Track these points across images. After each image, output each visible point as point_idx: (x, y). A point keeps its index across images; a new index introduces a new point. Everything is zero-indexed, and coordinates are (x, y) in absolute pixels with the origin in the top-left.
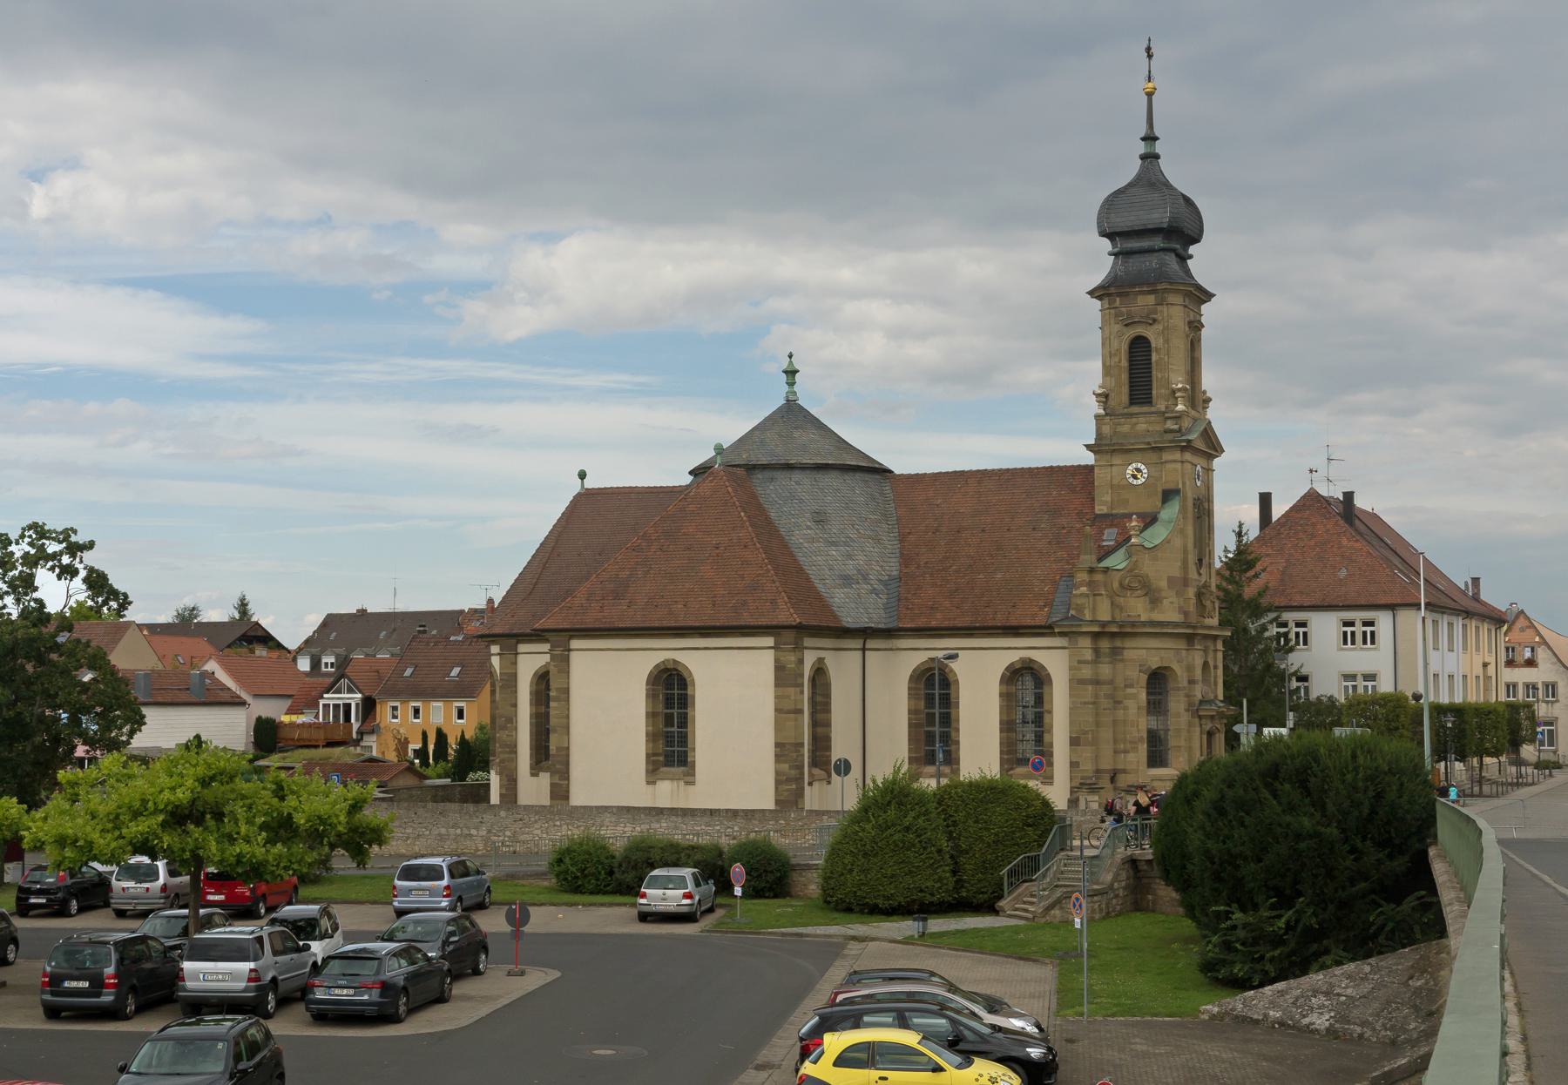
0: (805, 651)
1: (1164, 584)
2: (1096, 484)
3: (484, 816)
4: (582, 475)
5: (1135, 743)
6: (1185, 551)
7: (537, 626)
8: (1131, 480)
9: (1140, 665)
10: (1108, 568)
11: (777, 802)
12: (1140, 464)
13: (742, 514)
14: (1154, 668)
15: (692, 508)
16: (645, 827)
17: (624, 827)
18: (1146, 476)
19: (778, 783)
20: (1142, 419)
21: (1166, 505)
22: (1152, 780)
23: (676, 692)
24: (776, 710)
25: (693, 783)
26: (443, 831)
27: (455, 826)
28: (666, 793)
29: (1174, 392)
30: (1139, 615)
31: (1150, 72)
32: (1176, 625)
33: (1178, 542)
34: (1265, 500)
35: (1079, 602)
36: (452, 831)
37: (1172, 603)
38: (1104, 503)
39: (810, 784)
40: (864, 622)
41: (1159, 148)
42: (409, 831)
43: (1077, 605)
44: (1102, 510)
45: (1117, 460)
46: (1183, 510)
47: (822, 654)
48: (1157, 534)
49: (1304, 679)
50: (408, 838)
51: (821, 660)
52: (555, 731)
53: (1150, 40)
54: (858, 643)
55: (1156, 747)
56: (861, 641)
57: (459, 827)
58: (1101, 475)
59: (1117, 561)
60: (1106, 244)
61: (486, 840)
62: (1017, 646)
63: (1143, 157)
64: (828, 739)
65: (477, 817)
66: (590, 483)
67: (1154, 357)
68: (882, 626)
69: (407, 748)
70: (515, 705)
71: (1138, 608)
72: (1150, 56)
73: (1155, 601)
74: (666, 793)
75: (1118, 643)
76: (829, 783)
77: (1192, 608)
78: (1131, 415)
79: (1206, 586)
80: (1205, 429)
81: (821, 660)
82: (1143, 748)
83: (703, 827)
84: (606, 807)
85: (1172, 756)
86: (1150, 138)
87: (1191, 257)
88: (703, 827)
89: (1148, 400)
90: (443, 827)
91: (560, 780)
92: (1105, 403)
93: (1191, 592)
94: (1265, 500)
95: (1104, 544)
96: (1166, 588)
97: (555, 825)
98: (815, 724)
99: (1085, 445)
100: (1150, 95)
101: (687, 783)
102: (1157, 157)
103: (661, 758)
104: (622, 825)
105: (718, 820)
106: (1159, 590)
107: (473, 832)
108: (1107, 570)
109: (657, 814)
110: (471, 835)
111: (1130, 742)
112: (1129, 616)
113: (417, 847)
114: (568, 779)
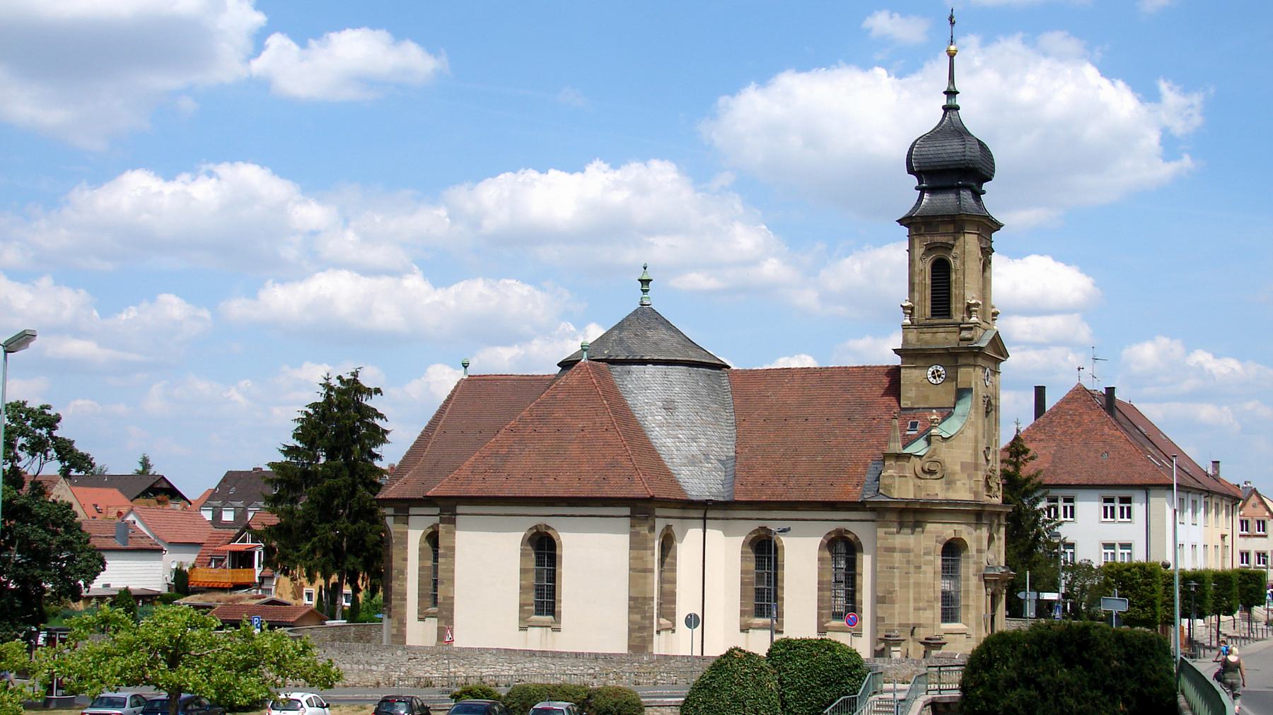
0: (656, 519)
1: (958, 468)
2: (902, 382)
3: (383, 654)
4: (465, 366)
5: (931, 602)
6: (976, 441)
7: (429, 494)
8: (931, 380)
9: (937, 537)
10: (911, 454)
11: (630, 647)
12: (939, 367)
13: (605, 402)
14: (948, 539)
15: (560, 396)
18: (944, 376)
19: (631, 631)
21: (960, 402)
23: (546, 552)
24: (630, 569)
25: (559, 630)
27: (358, 662)
28: (536, 639)
29: (969, 306)
31: (952, 37)
32: (967, 503)
33: (970, 433)
34: (1040, 392)
35: (886, 483)
36: (355, 666)
37: (964, 484)
38: (909, 399)
39: (658, 632)
40: (706, 496)
41: (959, 100)
43: (885, 484)
44: (906, 404)
46: (976, 406)
47: (670, 522)
48: (950, 427)
49: (1072, 546)
51: (668, 527)
52: (443, 583)
53: (952, 10)
54: (699, 513)
55: (948, 605)
56: (703, 512)
57: (361, 663)
58: (906, 375)
59: (919, 447)
60: (914, 180)
63: (947, 109)
64: (673, 594)
65: (377, 655)
67: (953, 276)
68: (721, 499)
69: (302, 591)
70: (405, 559)
71: (936, 490)
72: (952, 23)
73: (950, 483)
74: (536, 639)
75: (919, 518)
76: (674, 631)
77: (981, 488)
78: (932, 326)
79: (993, 471)
80: (994, 338)
81: (668, 527)
82: (938, 606)
84: (488, 649)
85: (962, 612)
86: (951, 93)
87: (984, 193)
89: (948, 314)
90: (348, 663)
92: (911, 315)
93: (981, 476)
94: (1040, 392)
95: (908, 433)
96: (960, 472)
98: (662, 581)
99: (894, 350)
100: (952, 56)
101: (554, 630)
102: (957, 108)
103: (533, 608)
106: (954, 474)
107: (374, 668)
108: (909, 456)
109: (531, 656)
111: (928, 601)
112: (928, 495)
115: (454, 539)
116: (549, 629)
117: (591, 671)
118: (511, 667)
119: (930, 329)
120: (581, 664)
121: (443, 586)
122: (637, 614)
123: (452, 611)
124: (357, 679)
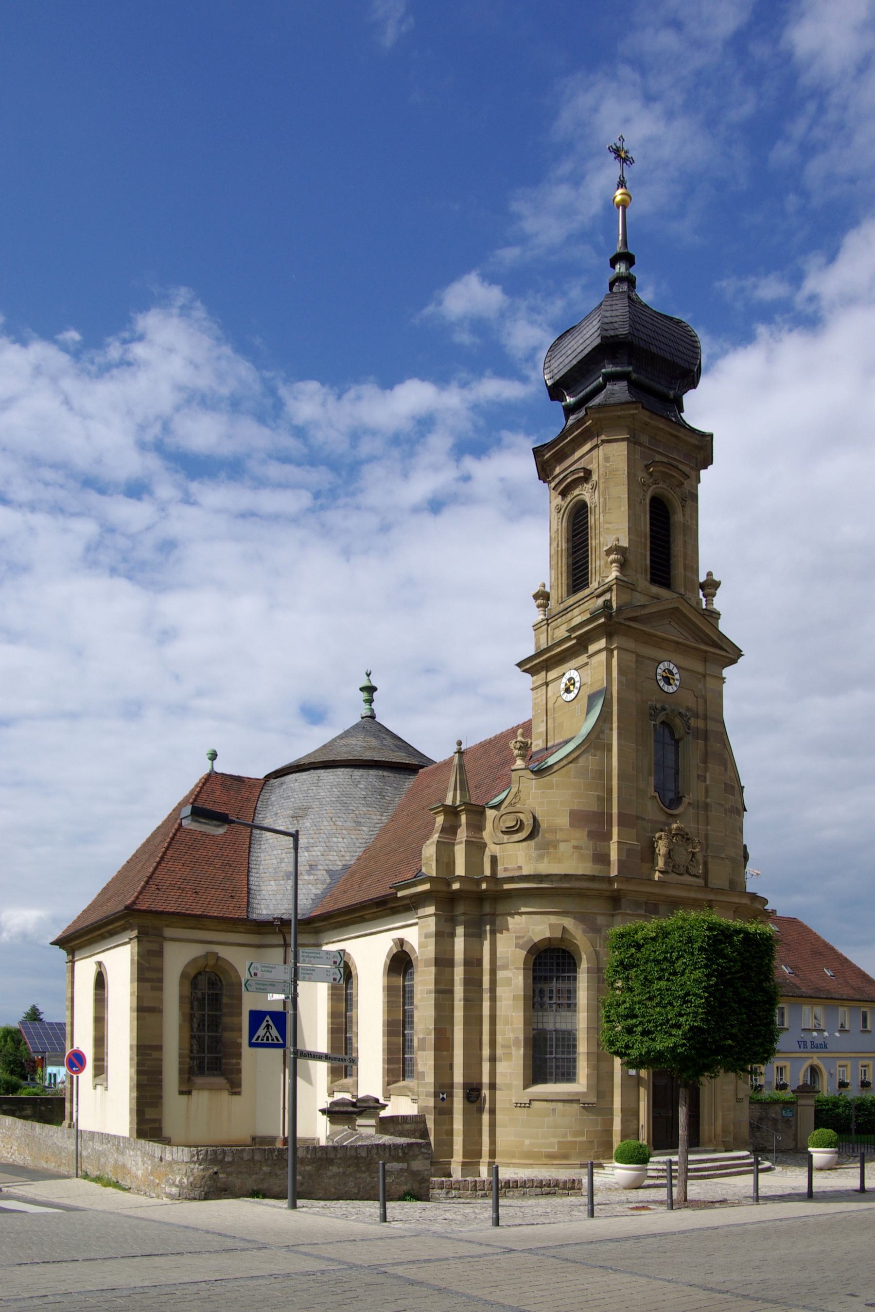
1: (564, 821)
9: (517, 938)
12: (572, 671)
14: (536, 941)
22: (530, 1100)
30: (520, 868)
37: (575, 847)
96: (567, 826)
106: (554, 830)
112: (506, 870)
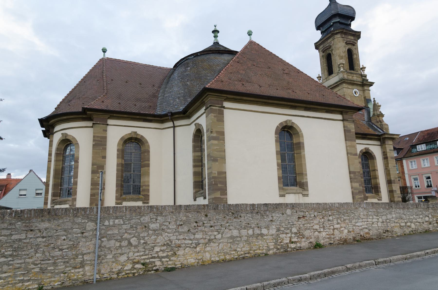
3: (273, 215)
4: (104, 51)
8: (355, 94)
16: (384, 218)
17: (373, 219)
18: (359, 94)
20: (355, 75)
26: (235, 233)
27: (248, 226)
35: (386, 127)
42: (199, 236)
43: (385, 128)
45: (350, 87)
50: (198, 244)
57: (251, 227)
61: (276, 238)
62: (364, 143)
65: (267, 216)
66: (108, 55)
70: (104, 157)
83: (415, 216)
88: (415, 216)
90: (235, 228)
91: (221, 195)
97: (329, 220)
104: (371, 217)
105: (421, 211)
107: (264, 231)
110: (262, 235)
113: (207, 254)
114: (226, 194)
115: (224, 125)
116: (301, 195)
117: (427, 219)
118: (378, 219)
119: (351, 75)
120: (420, 213)
121: (217, 163)
122: (371, 181)
123: (225, 183)
124: (246, 248)
